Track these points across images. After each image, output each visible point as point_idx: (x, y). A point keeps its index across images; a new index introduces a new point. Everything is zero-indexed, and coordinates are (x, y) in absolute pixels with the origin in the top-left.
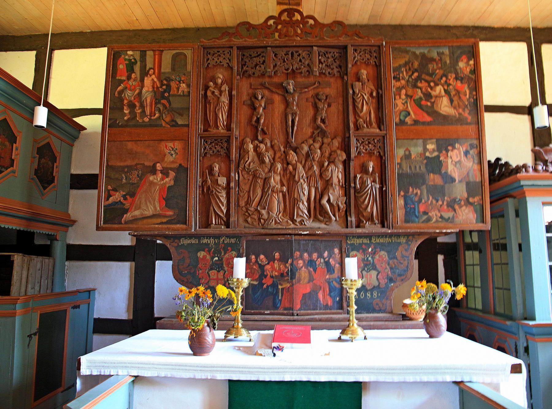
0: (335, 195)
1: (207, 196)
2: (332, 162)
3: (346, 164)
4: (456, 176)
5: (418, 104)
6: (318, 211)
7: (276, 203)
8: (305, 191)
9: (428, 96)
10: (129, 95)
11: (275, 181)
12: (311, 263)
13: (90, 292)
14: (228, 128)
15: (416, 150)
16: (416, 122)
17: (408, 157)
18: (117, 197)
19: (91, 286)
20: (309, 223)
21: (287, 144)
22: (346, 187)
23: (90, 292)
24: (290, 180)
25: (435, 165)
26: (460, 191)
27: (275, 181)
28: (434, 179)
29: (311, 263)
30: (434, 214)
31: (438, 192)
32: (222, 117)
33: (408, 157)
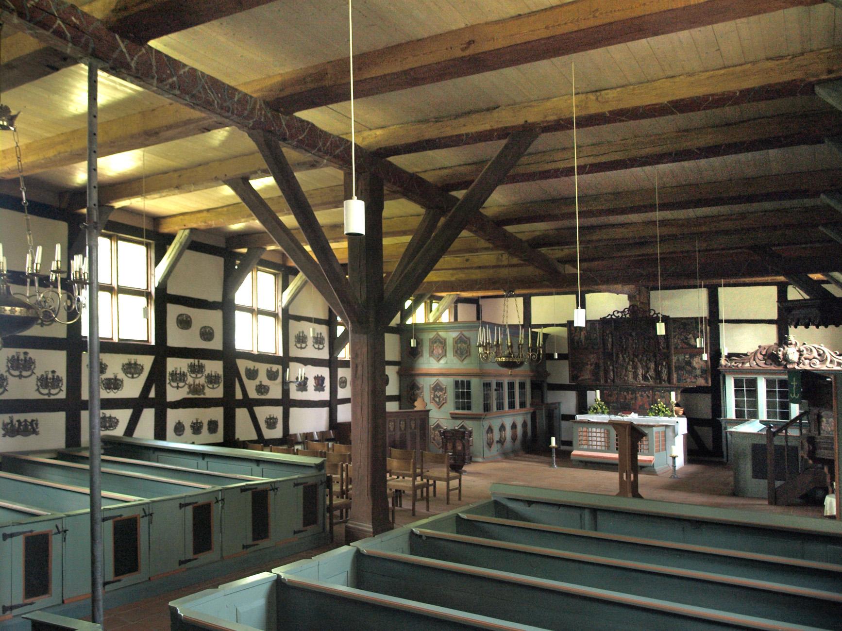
0: (652, 373)
1: (606, 372)
2: (650, 361)
3: (655, 362)
4: (697, 366)
5: (682, 340)
6: (645, 378)
7: (631, 375)
8: (640, 372)
9: (686, 339)
10: (576, 338)
11: (630, 367)
12: (642, 396)
13: (559, 403)
14: (612, 348)
15: (681, 357)
16: (682, 348)
17: (678, 360)
18: (575, 372)
19: (559, 400)
20: (642, 382)
21: (634, 355)
22: (656, 370)
23: (559, 403)
24: (635, 367)
25: (689, 363)
26: (698, 372)
27: (630, 367)
28: (688, 368)
29: (642, 396)
30: (688, 380)
31: (690, 372)
32: (610, 346)
33: (678, 360)
